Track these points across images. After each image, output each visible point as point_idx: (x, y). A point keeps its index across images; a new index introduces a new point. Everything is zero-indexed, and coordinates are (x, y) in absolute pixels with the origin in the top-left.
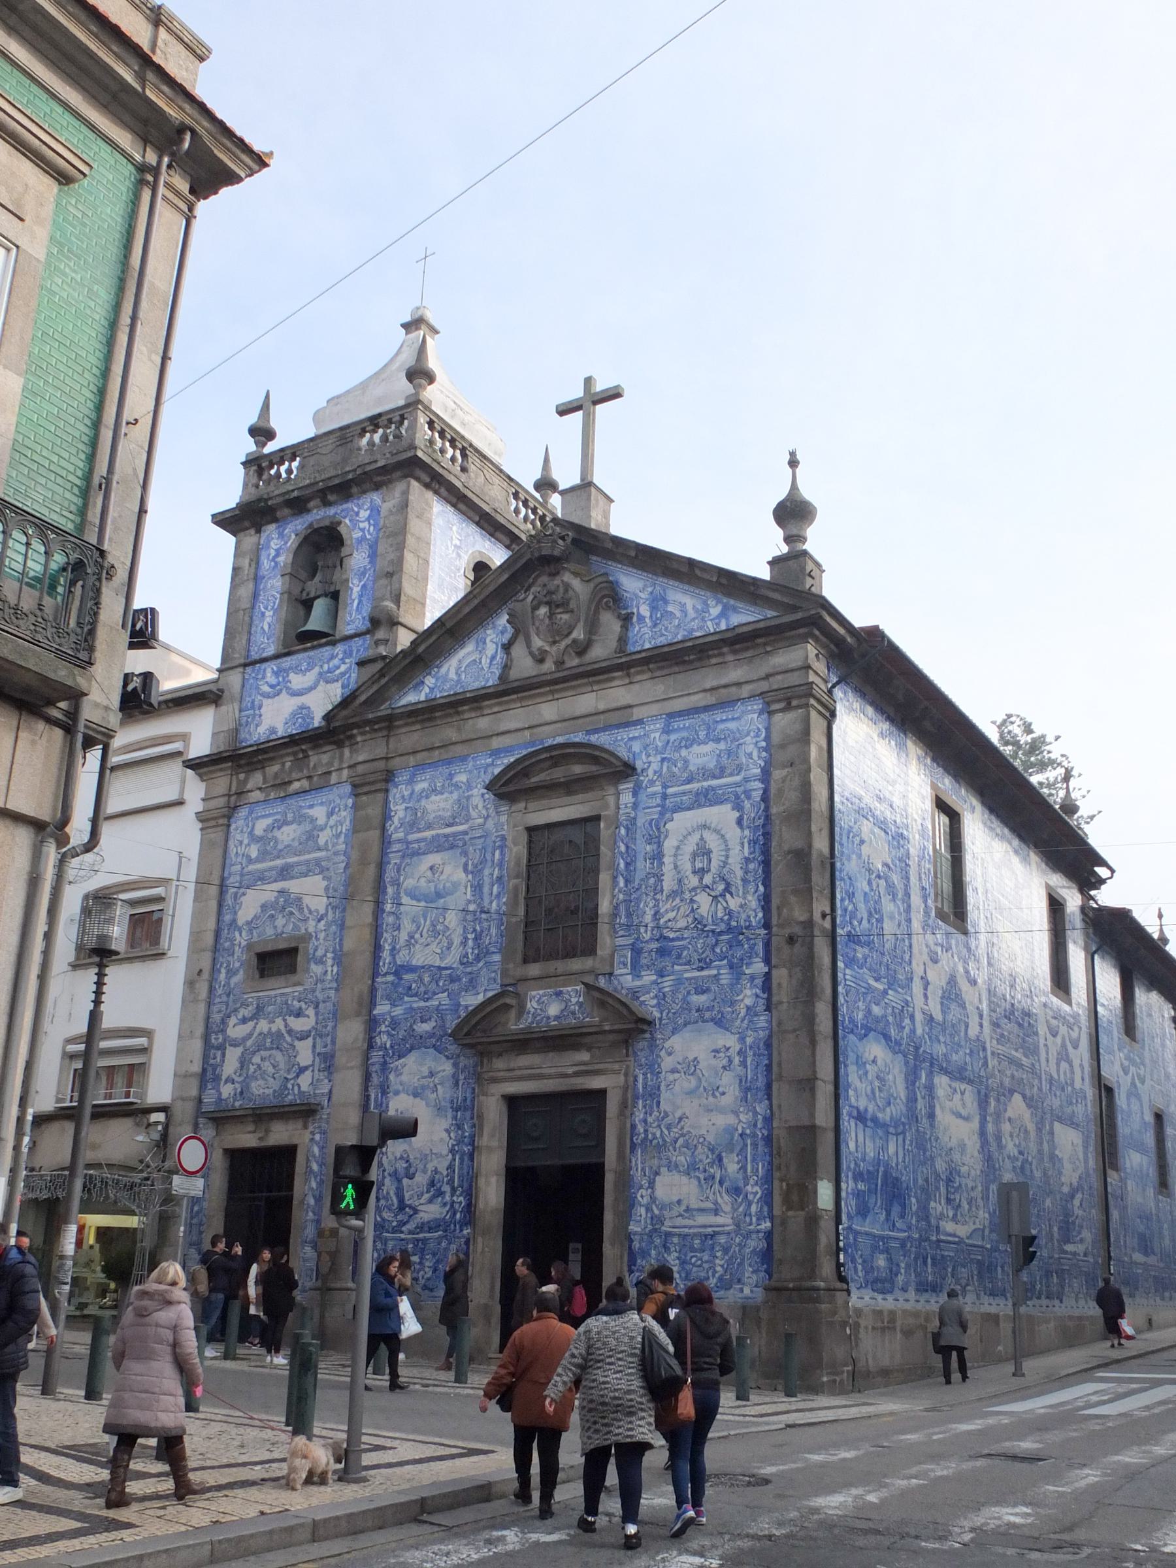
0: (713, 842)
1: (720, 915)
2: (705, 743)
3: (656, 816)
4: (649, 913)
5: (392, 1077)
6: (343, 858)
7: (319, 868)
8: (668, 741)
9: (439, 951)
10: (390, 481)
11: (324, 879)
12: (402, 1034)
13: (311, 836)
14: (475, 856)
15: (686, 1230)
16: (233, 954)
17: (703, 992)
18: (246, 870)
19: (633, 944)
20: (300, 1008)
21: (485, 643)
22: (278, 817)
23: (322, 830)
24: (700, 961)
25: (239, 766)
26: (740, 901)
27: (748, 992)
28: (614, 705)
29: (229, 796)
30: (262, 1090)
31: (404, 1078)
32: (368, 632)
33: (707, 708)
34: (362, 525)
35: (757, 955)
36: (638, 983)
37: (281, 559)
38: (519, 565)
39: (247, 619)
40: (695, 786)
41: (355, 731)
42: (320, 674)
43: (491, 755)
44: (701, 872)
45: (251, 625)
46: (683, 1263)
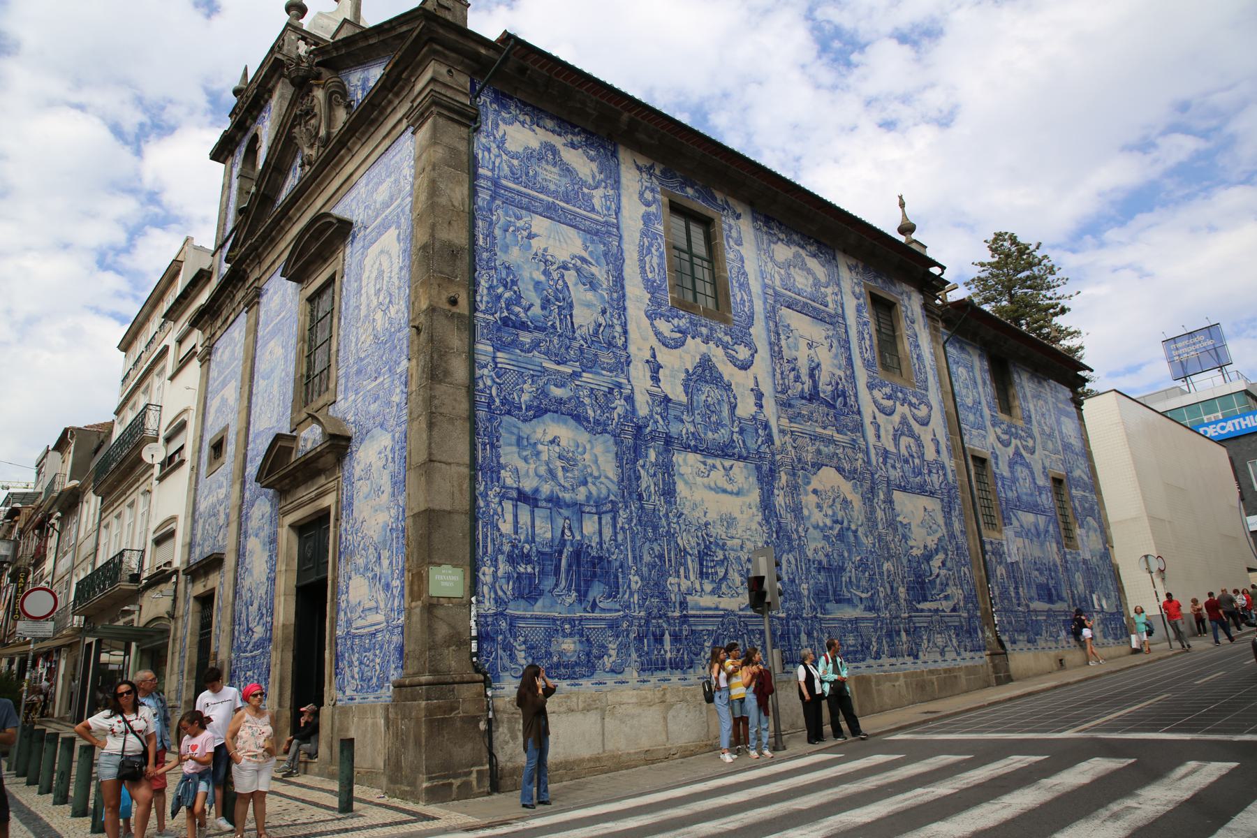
0: (386, 266)
2: (384, 181)
4: (354, 340)
13: (233, 352)
15: (362, 630)
26: (396, 307)
30: (207, 551)
36: (346, 405)
40: (379, 220)
46: (361, 663)
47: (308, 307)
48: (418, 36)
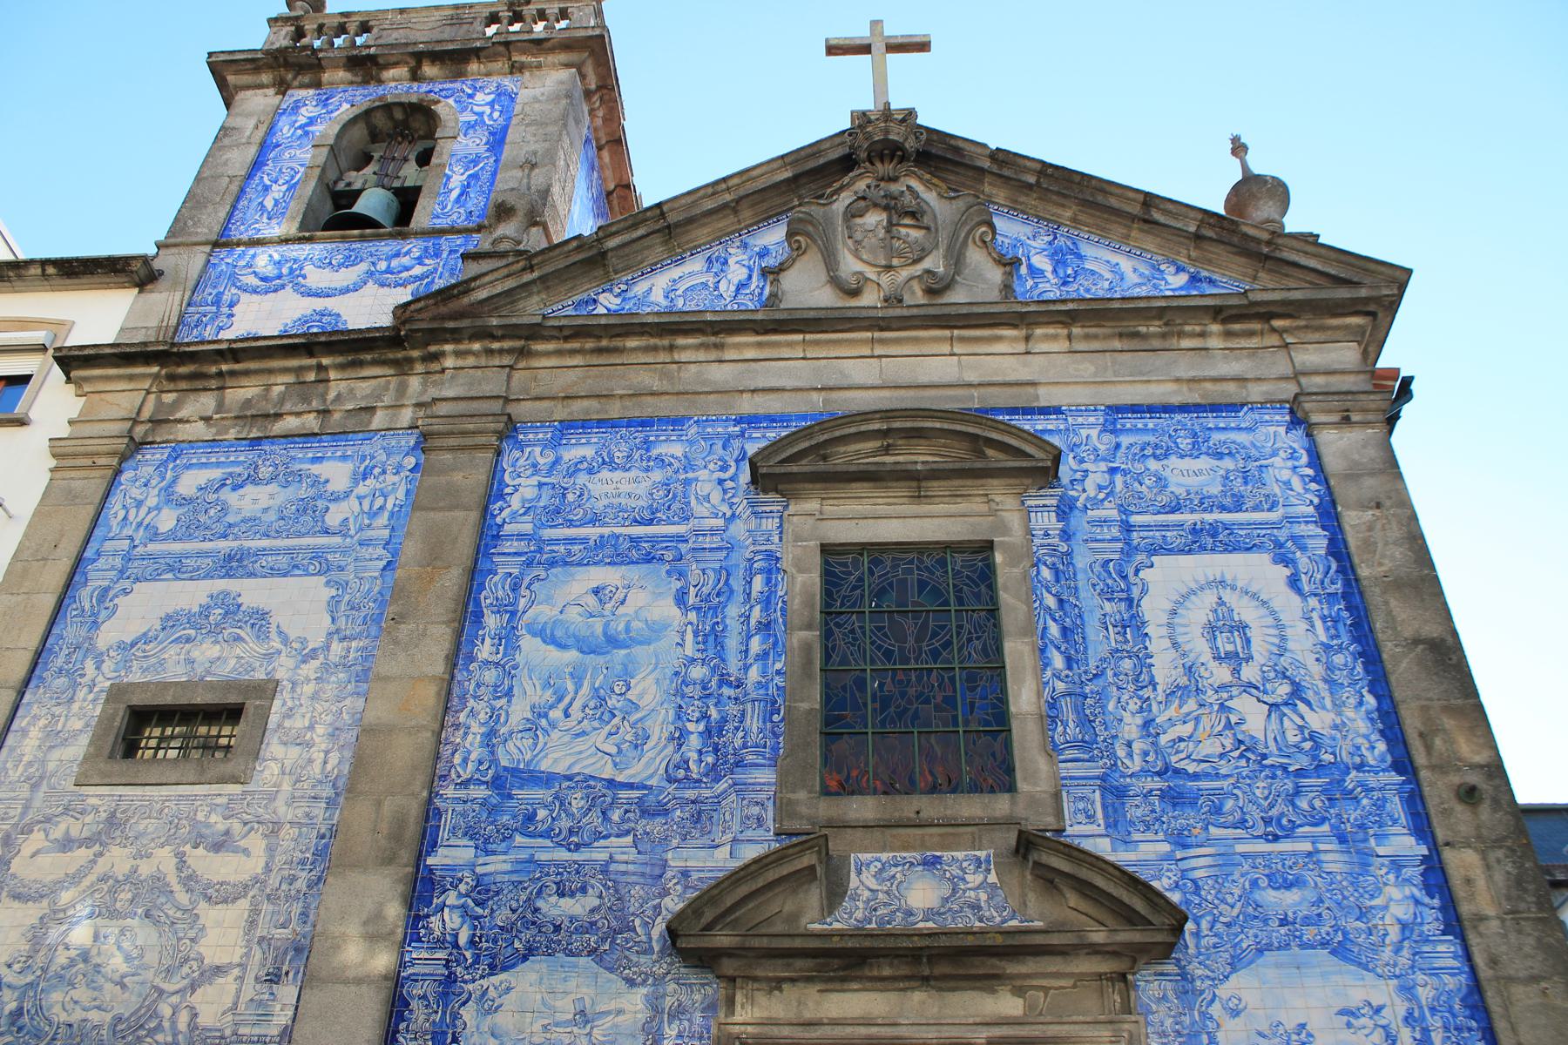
0: (1246, 612)
1: (1292, 737)
3: (1116, 556)
5: (468, 1014)
6: (380, 551)
7: (320, 563)
8: (1118, 446)
9: (614, 750)
10: (539, 66)
11: (328, 583)
12: (502, 916)
13: (309, 511)
14: (701, 577)
16: (71, 700)
17: (1289, 886)
18: (140, 550)
19: (1103, 778)
20: (227, 833)
21: (726, 262)
22: (238, 470)
23: (337, 499)
24: (1267, 822)
25: (172, 378)
27: (1394, 893)
28: (999, 379)
29: (135, 422)
31: (503, 1019)
32: (479, 229)
33: (1184, 408)
34: (476, 109)
35: (1395, 821)
37: (317, 129)
38: (811, 164)
39: (234, 188)
40: (1188, 518)
41: (448, 348)
42: (370, 274)
43: (738, 422)
44: (1235, 660)
45: (238, 199)
47: (816, 559)
48: (1367, 300)
